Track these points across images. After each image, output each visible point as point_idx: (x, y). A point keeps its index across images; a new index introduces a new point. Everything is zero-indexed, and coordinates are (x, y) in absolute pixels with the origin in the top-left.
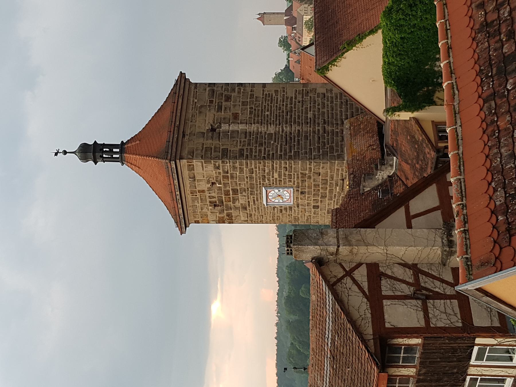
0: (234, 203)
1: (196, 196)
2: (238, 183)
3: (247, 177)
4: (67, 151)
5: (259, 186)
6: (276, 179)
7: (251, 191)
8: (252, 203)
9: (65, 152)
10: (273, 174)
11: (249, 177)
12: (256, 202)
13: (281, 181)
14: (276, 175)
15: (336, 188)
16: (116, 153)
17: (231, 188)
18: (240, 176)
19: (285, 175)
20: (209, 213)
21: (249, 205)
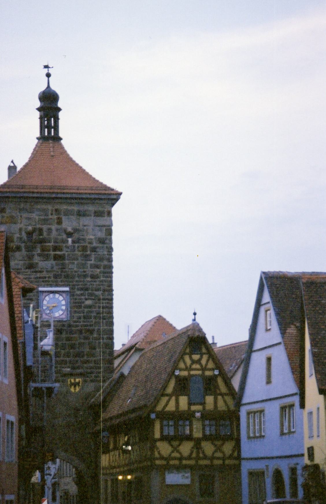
0: (39, 255)
1: (52, 214)
2: (76, 262)
3: (85, 272)
4: (50, 78)
5: (71, 284)
6: (84, 303)
7: (61, 275)
8: (38, 275)
9: (48, 75)
10: (92, 299)
11: (85, 273)
12: (41, 280)
13: (80, 307)
14: (89, 302)
15: (69, 367)
16: (49, 132)
17: (66, 253)
18: (88, 264)
19: (91, 312)
20: (19, 226)
21: (36, 272)
